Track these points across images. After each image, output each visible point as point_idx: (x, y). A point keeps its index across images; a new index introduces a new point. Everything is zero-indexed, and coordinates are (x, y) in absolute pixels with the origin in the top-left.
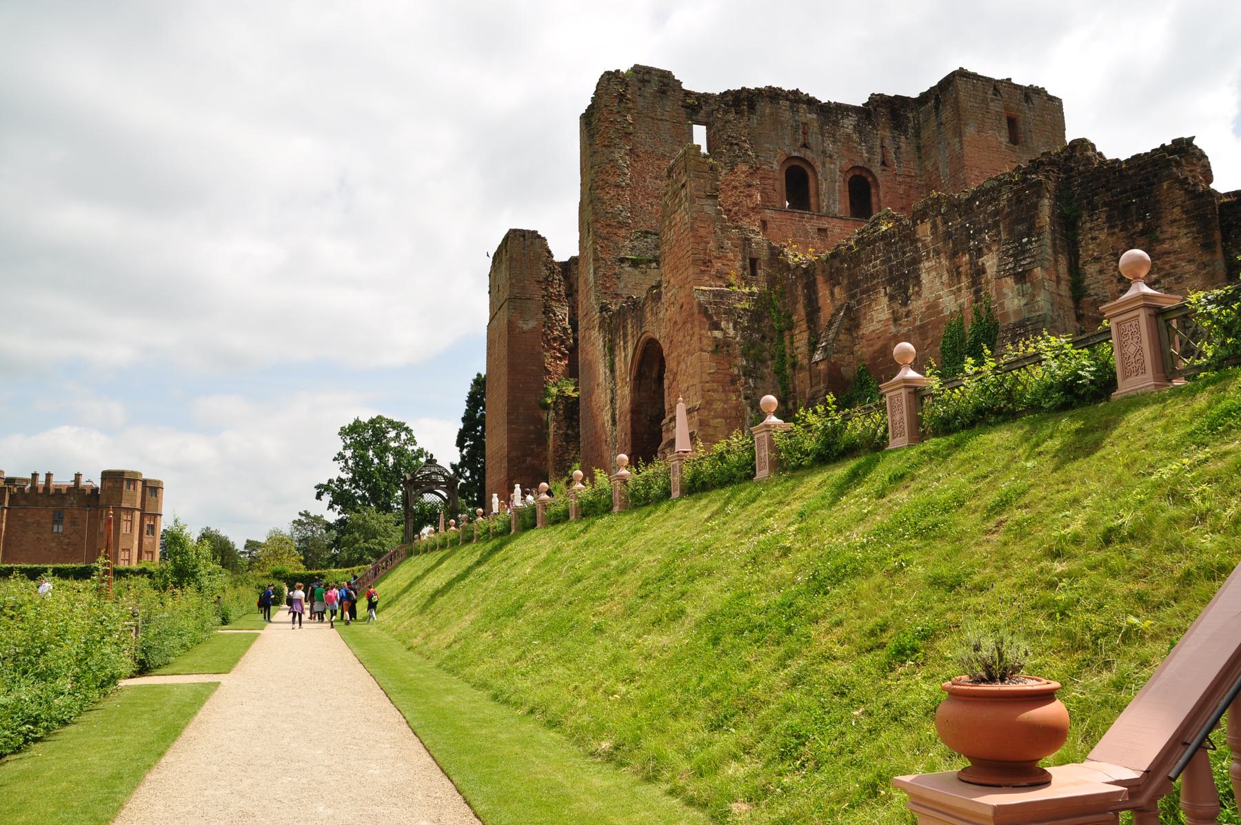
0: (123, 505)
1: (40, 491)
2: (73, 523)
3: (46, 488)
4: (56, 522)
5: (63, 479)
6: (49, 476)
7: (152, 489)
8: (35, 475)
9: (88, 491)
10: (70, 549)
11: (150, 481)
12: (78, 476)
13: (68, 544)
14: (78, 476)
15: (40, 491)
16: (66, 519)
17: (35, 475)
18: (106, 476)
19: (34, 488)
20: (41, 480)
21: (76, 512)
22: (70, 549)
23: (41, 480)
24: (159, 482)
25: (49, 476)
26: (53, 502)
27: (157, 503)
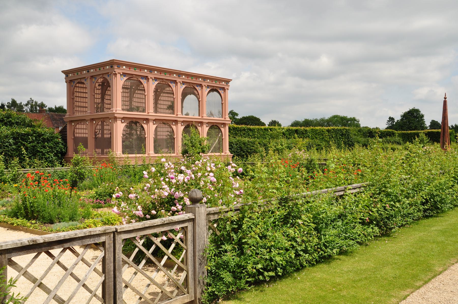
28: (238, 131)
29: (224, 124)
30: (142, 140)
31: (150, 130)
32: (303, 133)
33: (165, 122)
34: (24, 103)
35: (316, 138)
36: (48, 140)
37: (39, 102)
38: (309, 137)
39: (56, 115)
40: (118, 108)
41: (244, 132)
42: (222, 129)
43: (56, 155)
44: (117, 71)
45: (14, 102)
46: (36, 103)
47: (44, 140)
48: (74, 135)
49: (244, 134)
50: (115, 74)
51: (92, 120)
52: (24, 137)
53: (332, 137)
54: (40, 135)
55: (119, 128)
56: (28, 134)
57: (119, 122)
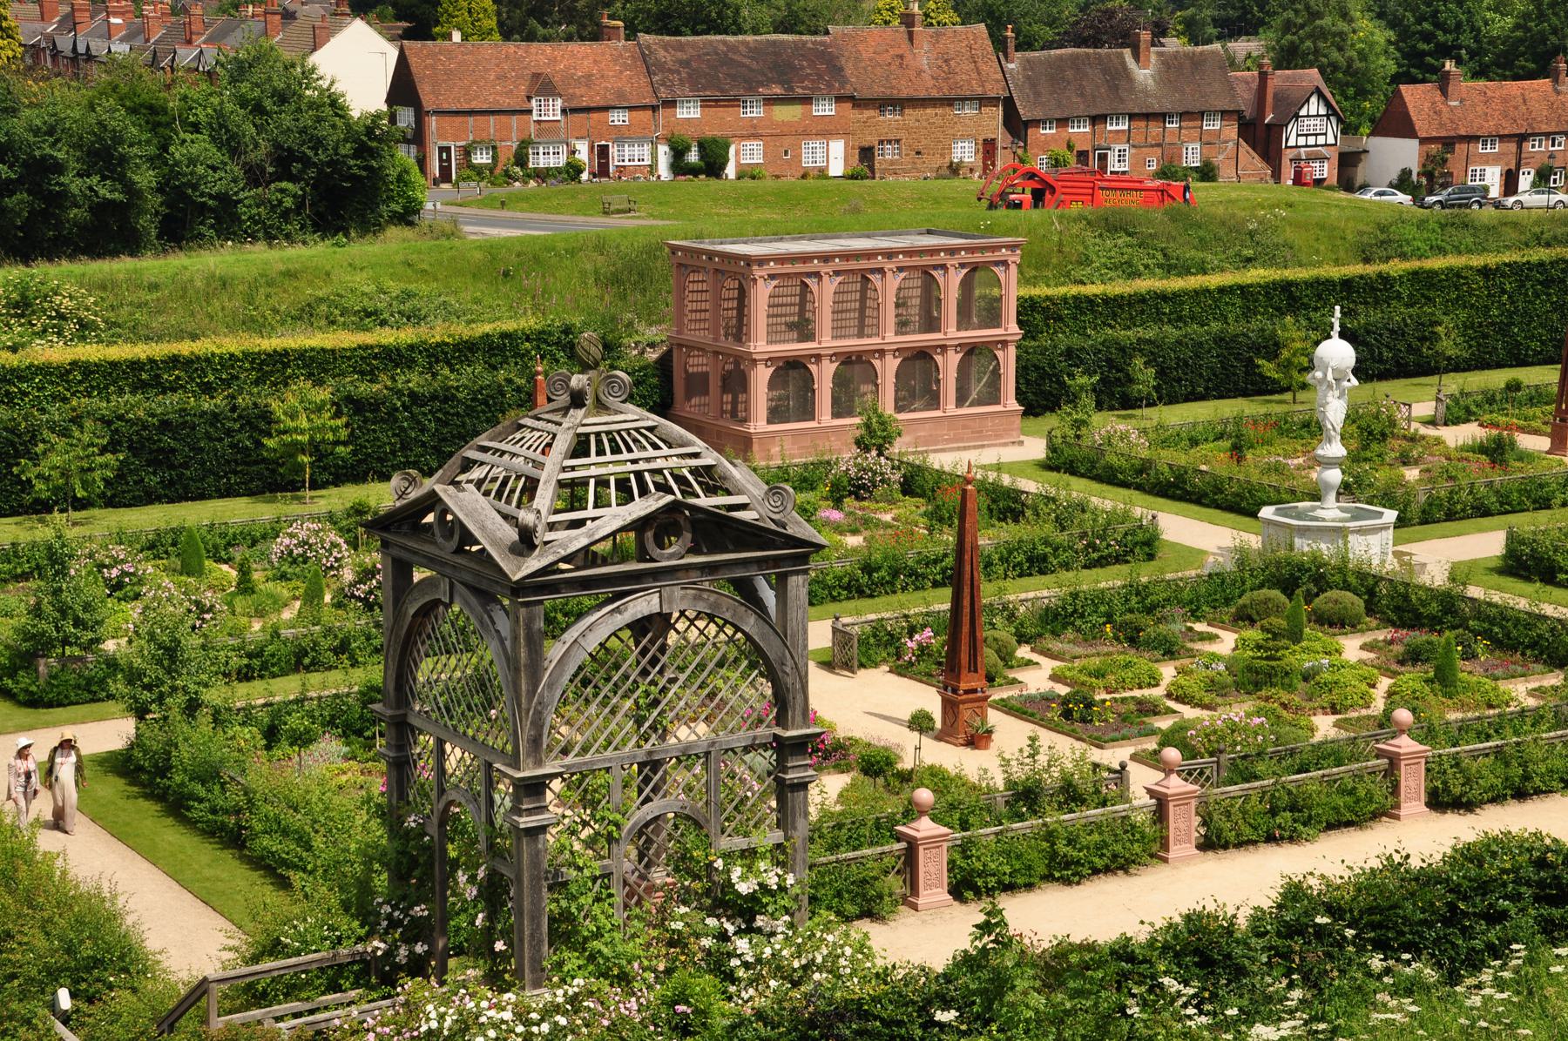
28: (1120, 306)
29: (1005, 343)
31: (824, 376)
32: (1373, 289)
35: (1428, 299)
38: (1399, 297)
39: (665, 47)
40: (760, 345)
41: (1138, 307)
42: (999, 354)
44: (758, 272)
48: (686, 371)
49: (1142, 312)
50: (755, 280)
51: (716, 353)
53: (1504, 292)
57: (761, 367)
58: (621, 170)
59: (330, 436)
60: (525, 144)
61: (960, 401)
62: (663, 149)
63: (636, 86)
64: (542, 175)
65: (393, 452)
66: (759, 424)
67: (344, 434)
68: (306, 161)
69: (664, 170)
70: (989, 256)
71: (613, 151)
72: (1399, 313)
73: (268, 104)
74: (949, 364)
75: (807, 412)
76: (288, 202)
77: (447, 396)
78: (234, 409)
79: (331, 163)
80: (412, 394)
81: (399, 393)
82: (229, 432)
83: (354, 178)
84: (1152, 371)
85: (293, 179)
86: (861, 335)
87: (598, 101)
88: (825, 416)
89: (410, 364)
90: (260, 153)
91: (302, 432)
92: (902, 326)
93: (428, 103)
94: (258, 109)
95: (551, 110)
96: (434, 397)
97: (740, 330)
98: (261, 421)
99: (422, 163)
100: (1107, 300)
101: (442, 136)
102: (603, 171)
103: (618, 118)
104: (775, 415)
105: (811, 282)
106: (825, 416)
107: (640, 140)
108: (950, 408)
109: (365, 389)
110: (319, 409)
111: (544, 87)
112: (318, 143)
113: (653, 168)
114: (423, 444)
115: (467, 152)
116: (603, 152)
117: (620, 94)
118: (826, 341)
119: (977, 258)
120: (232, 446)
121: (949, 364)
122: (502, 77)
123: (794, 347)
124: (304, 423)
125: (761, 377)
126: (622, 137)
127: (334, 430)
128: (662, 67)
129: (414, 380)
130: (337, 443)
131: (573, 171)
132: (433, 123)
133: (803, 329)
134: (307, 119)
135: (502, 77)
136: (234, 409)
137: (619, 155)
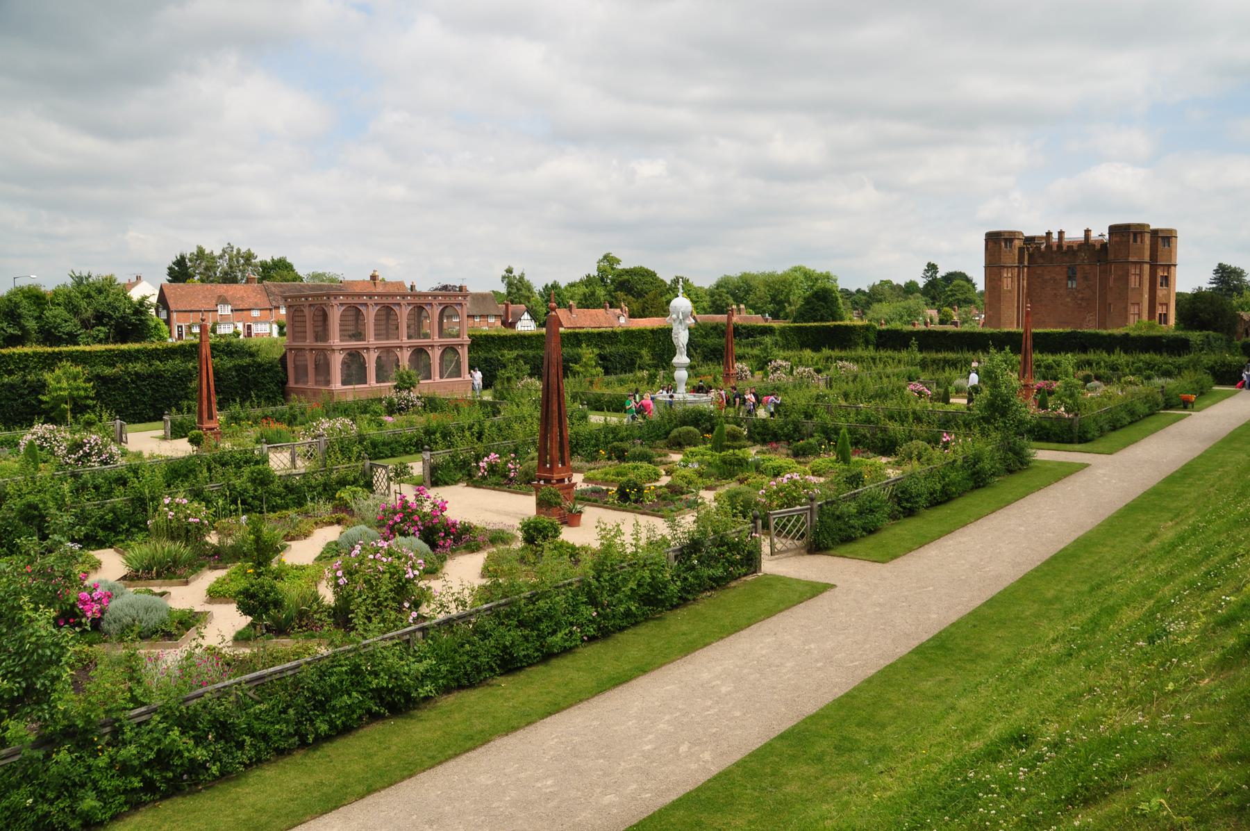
0: (1131, 259)
1: (1055, 248)
2: (1086, 278)
3: (1060, 246)
4: (1070, 278)
5: (1074, 234)
6: (1061, 233)
7: (1163, 239)
8: (1049, 234)
9: (1098, 247)
10: (1084, 304)
11: (1162, 231)
12: (1087, 232)
13: (1082, 299)
14: (1087, 232)
15: (1055, 248)
16: (1079, 275)
17: (1049, 234)
18: (1113, 230)
19: (1049, 246)
20: (1055, 236)
21: (1087, 268)
22: (1084, 304)
23: (1055, 236)
24: (1170, 231)
25: (1061, 233)
26: (1066, 259)
27: (1171, 253)
30: (363, 367)
31: (371, 359)
33: (388, 350)
34: (217, 253)
36: (268, 370)
37: (243, 250)
40: (336, 341)
43: (276, 385)
44: (334, 302)
45: (201, 251)
46: (239, 251)
47: (265, 370)
52: (245, 369)
54: (260, 365)
55: (337, 360)
56: (249, 365)
57: (337, 354)
58: (257, 335)
59: (82, 393)
60: (215, 324)
61: (441, 377)
62: (275, 328)
63: (264, 302)
64: (221, 336)
65: (127, 408)
66: (337, 385)
67: (92, 394)
68: (110, 317)
69: (275, 334)
70: (452, 300)
71: (253, 327)
72: (622, 349)
73: (93, 294)
74: (435, 355)
75: (363, 379)
76: (102, 335)
77: (158, 375)
78: (25, 382)
79: (122, 317)
80: (137, 374)
81: (129, 374)
82: (21, 396)
83: (133, 324)
84: (528, 367)
85: (104, 325)
86: (388, 339)
87: (247, 307)
88: (372, 381)
89: (137, 359)
90: (89, 313)
91: (65, 389)
92: (409, 337)
93: (172, 307)
94: (89, 296)
95: (225, 310)
96: (150, 376)
97: (323, 334)
98: (42, 386)
99: (170, 332)
100: (500, 337)
101: (178, 320)
102: (249, 335)
103: (255, 314)
104: (344, 383)
105: (362, 309)
106: (372, 381)
107: (265, 322)
108: (437, 378)
109: (108, 371)
110: (75, 378)
111: (223, 301)
112: (115, 309)
113: (270, 334)
114: (145, 403)
115: (190, 327)
116: (249, 327)
117: (256, 304)
118: (371, 341)
119: (448, 301)
120: (23, 404)
121: (435, 355)
122: (205, 297)
123: (354, 344)
124: (65, 385)
125: (337, 360)
126: (257, 321)
127: (86, 390)
128: (273, 294)
129: (138, 367)
130: (87, 397)
131: (237, 334)
132: (174, 315)
133: (359, 335)
134: (110, 299)
135: (205, 297)
136: (25, 382)
137: (258, 329)
